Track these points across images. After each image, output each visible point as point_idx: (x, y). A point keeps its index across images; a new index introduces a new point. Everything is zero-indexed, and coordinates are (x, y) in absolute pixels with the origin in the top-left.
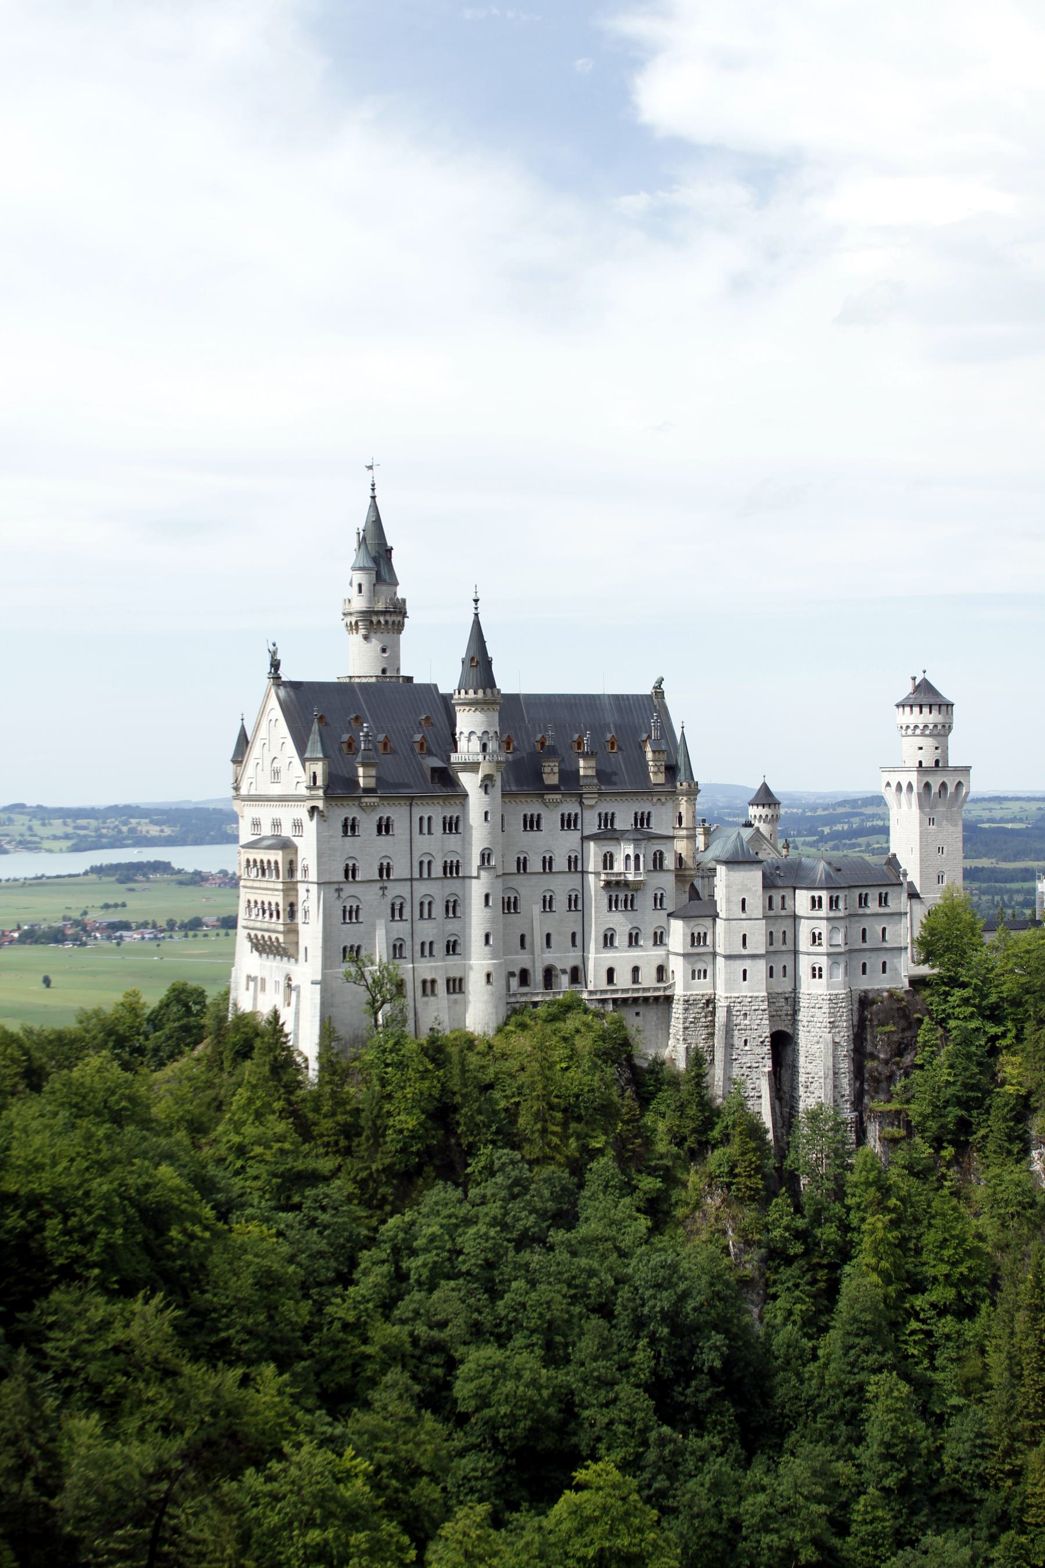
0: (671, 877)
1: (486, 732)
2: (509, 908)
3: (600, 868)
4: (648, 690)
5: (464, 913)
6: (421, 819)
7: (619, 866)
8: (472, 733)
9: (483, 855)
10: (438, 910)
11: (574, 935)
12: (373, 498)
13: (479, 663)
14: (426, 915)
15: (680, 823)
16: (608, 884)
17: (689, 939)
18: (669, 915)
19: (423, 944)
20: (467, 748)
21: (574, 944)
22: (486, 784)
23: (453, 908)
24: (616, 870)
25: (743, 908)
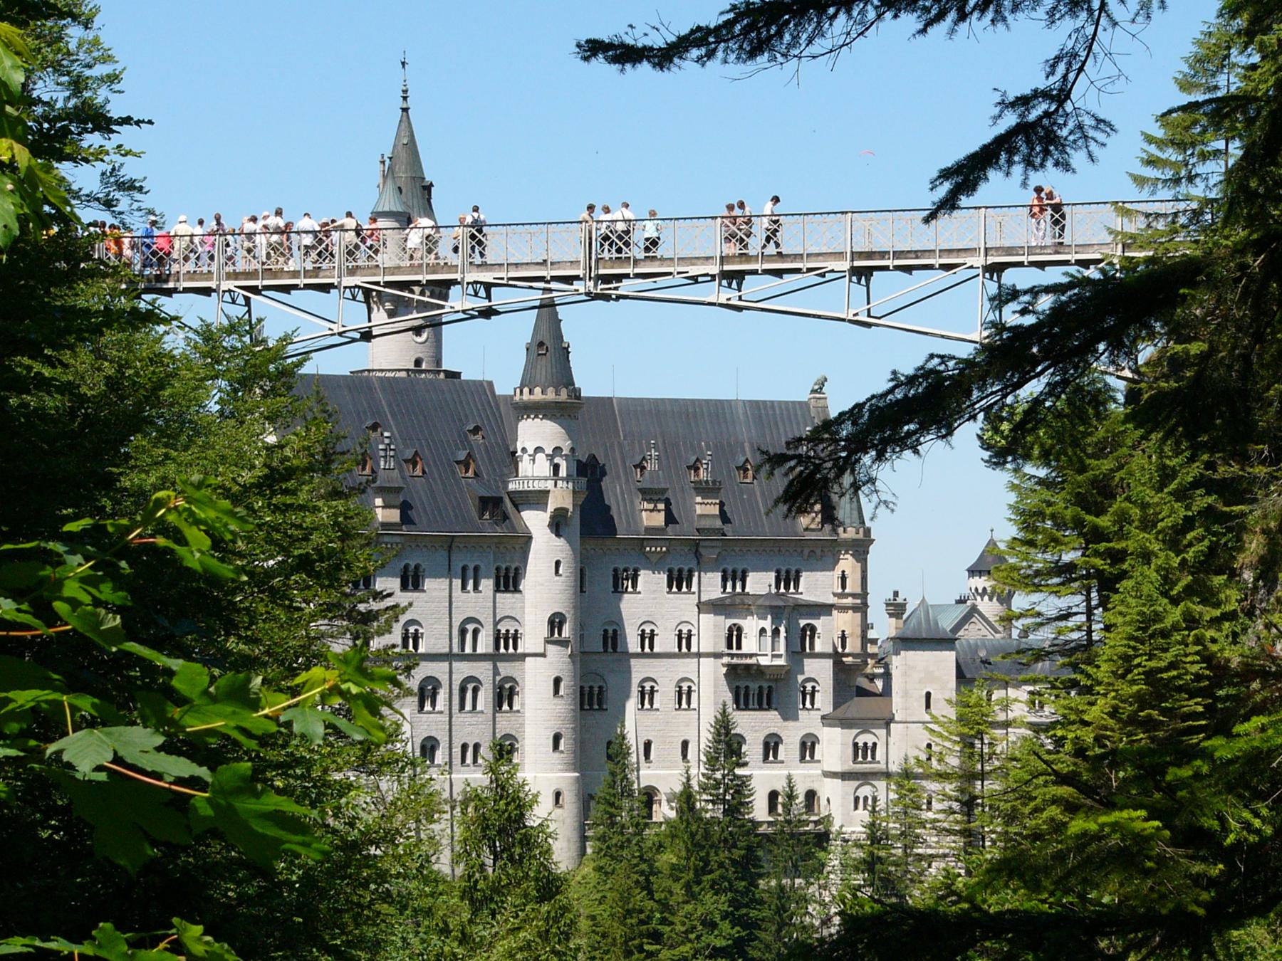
0: (828, 664)
1: (557, 450)
2: (591, 704)
3: (722, 648)
4: (804, 396)
5: (523, 705)
6: (464, 569)
7: (749, 645)
8: (539, 450)
9: (551, 623)
10: (485, 698)
11: (685, 744)
12: (405, 110)
13: (550, 351)
14: (468, 707)
15: (844, 587)
16: (733, 673)
17: (850, 750)
18: (823, 717)
19: (464, 747)
20: (533, 471)
21: (685, 755)
22: (558, 524)
23: (505, 694)
24: (745, 650)
25: (928, 706)
